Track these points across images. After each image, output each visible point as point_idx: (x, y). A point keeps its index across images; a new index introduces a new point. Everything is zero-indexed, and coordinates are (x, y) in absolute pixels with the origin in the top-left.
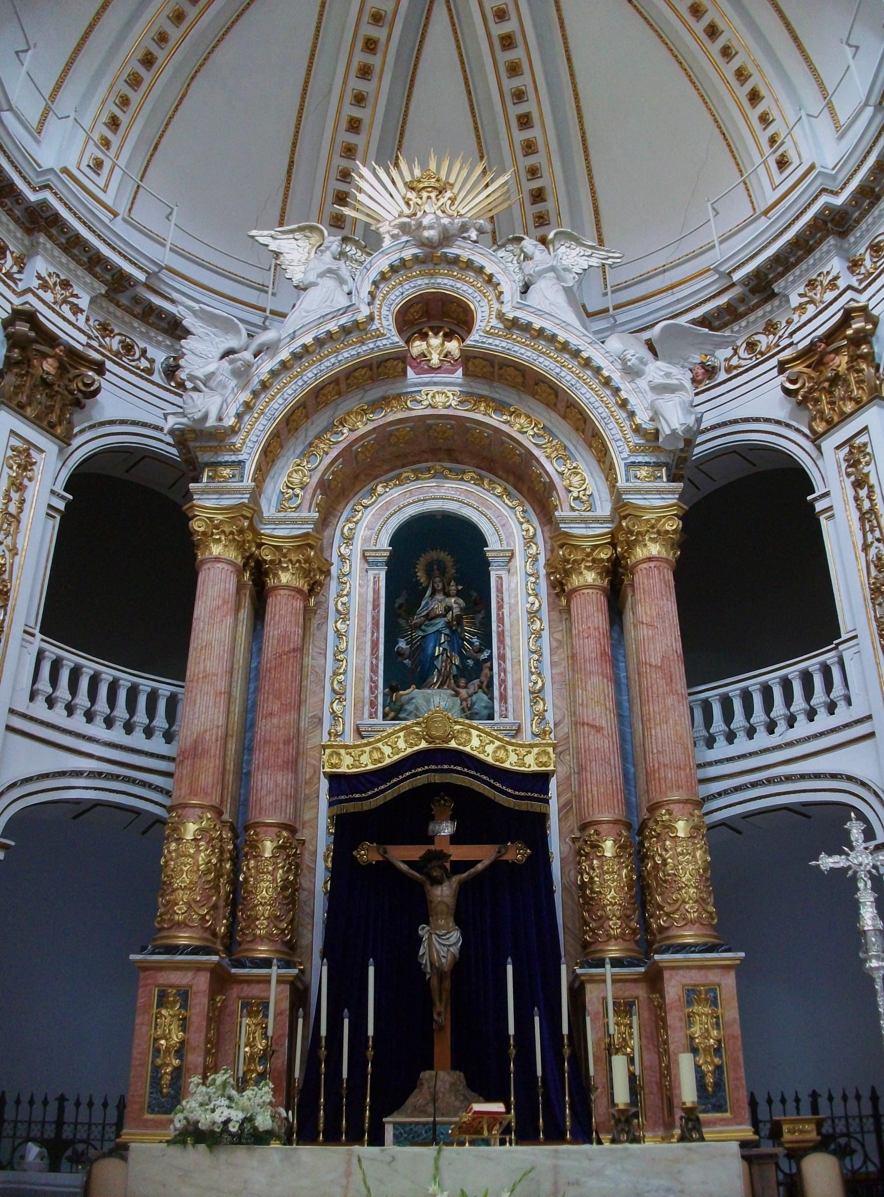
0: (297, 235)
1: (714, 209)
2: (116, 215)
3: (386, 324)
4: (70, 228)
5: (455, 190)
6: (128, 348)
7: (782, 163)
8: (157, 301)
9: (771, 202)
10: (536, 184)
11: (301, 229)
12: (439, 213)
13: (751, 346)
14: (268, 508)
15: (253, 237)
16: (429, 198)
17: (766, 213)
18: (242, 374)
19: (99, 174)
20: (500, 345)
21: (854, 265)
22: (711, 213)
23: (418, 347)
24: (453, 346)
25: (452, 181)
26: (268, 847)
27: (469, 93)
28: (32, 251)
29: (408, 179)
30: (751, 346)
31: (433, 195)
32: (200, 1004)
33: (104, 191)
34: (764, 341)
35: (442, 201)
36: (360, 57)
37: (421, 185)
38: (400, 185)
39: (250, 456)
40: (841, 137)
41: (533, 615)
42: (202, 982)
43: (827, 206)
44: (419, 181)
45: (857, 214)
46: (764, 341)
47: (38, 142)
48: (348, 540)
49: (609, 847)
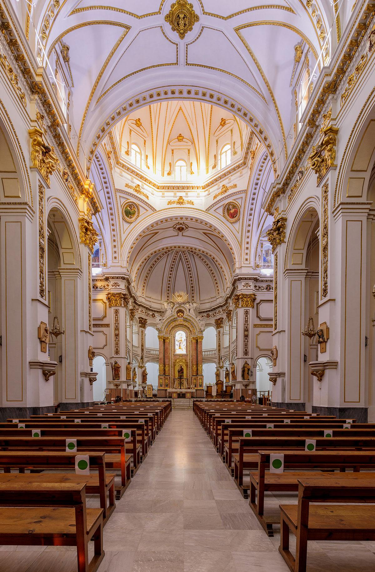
3: (176, 314)
6: (148, 314)
8: (151, 309)
13: (213, 315)
14: (165, 334)
18: (162, 322)
20: (187, 317)
21: (223, 310)
23: (179, 314)
24: (182, 314)
26: (167, 366)
28: (139, 308)
30: (213, 315)
32: (163, 379)
34: (215, 314)
36: (171, 269)
39: (163, 330)
41: (190, 343)
42: (163, 377)
46: (215, 314)
48: (172, 335)
49: (195, 366)
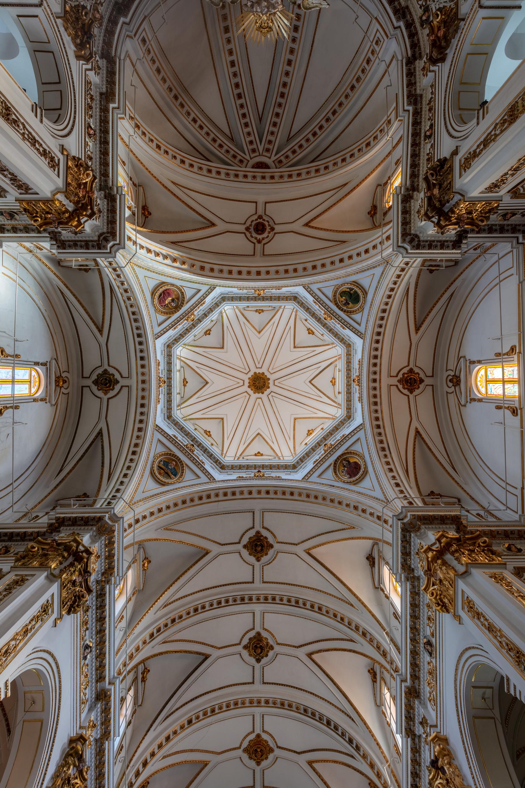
0: (312, 5)
1: (164, 19)
2: (376, 18)
4: (391, 8)
5: (255, 27)
7: (144, 41)
9: (144, 22)
10: (227, 35)
11: (310, 8)
12: (261, 15)
15: (328, 4)
16: (265, 23)
17: (145, 17)
19: (378, 38)
22: (165, 17)
25: (257, 32)
27: (251, 77)
29: (272, 32)
31: (263, 25)
33: (378, 30)
35: (260, 22)
37: (267, 29)
38: (274, 30)
40: (127, 52)
43: (126, 16)
44: (268, 31)
45: (114, 13)
47: (395, 52)
